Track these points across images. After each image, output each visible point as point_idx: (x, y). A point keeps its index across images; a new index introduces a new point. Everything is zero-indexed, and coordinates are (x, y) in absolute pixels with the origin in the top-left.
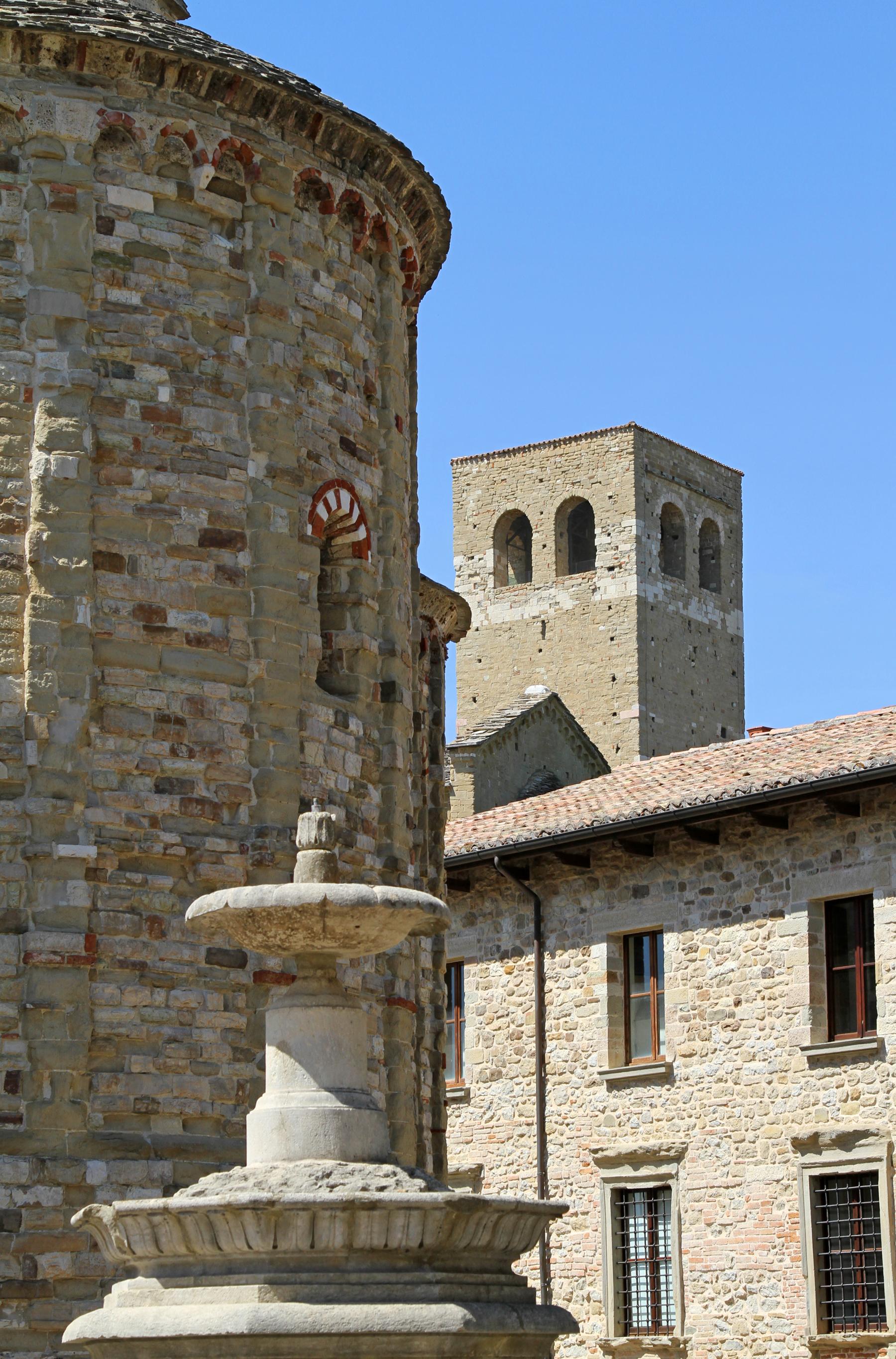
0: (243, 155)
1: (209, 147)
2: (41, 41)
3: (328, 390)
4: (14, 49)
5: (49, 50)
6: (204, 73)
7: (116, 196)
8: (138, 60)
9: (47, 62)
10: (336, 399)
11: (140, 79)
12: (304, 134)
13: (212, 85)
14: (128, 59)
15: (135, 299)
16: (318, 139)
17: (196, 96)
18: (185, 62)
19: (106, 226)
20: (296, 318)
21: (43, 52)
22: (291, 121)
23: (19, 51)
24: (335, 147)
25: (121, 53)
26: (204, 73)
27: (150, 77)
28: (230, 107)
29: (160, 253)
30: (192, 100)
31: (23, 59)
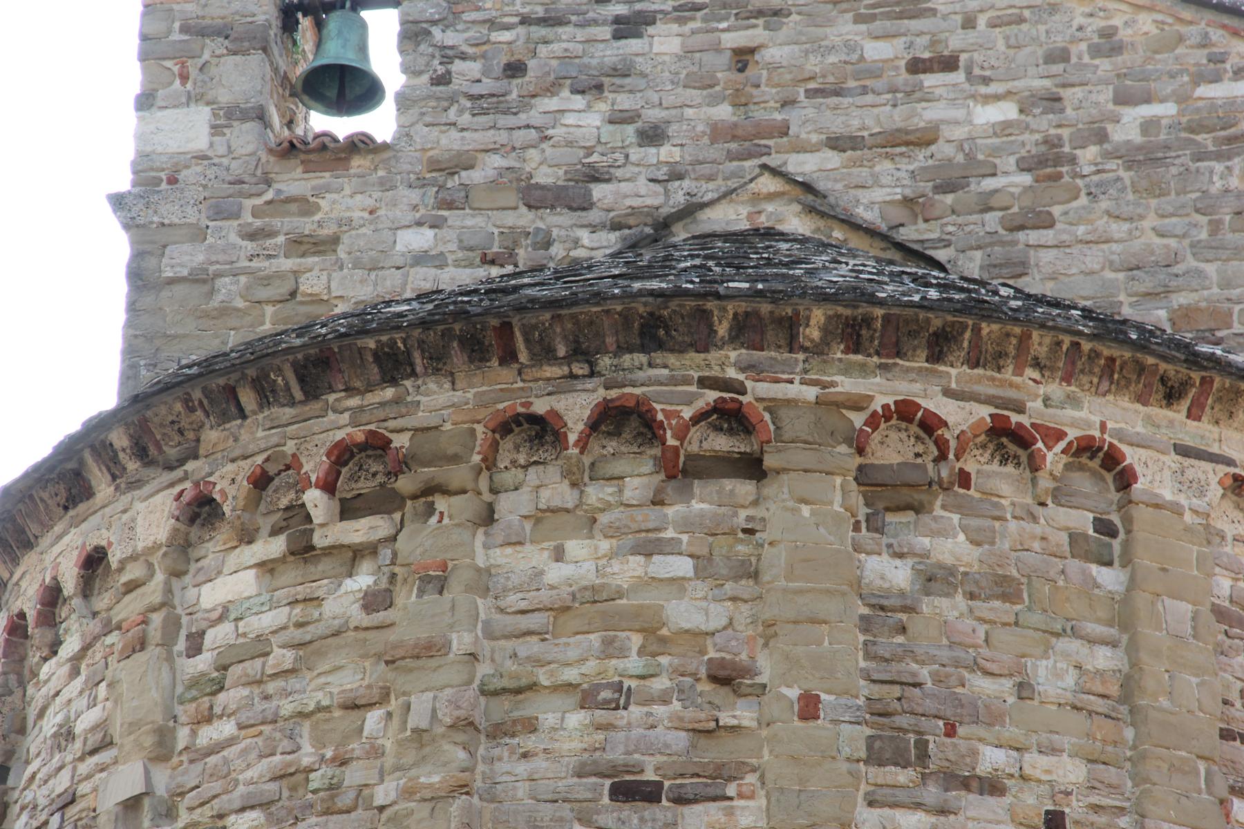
0: (377, 445)
1: (314, 465)
2: (111, 445)
3: (576, 719)
4: (100, 470)
5: (124, 450)
6: (280, 370)
7: (212, 596)
8: (201, 403)
9: (132, 465)
10: (599, 727)
11: (219, 425)
12: (495, 362)
13: (302, 380)
14: (192, 410)
15: (226, 728)
16: (523, 357)
17: (292, 403)
18: (251, 372)
19: (195, 646)
20: (461, 642)
21: (121, 455)
22: (458, 358)
23: (104, 468)
24: (562, 351)
25: (178, 407)
26: (280, 370)
27: (224, 418)
28: (350, 390)
29: (260, 647)
30: (288, 413)
31: (114, 477)
